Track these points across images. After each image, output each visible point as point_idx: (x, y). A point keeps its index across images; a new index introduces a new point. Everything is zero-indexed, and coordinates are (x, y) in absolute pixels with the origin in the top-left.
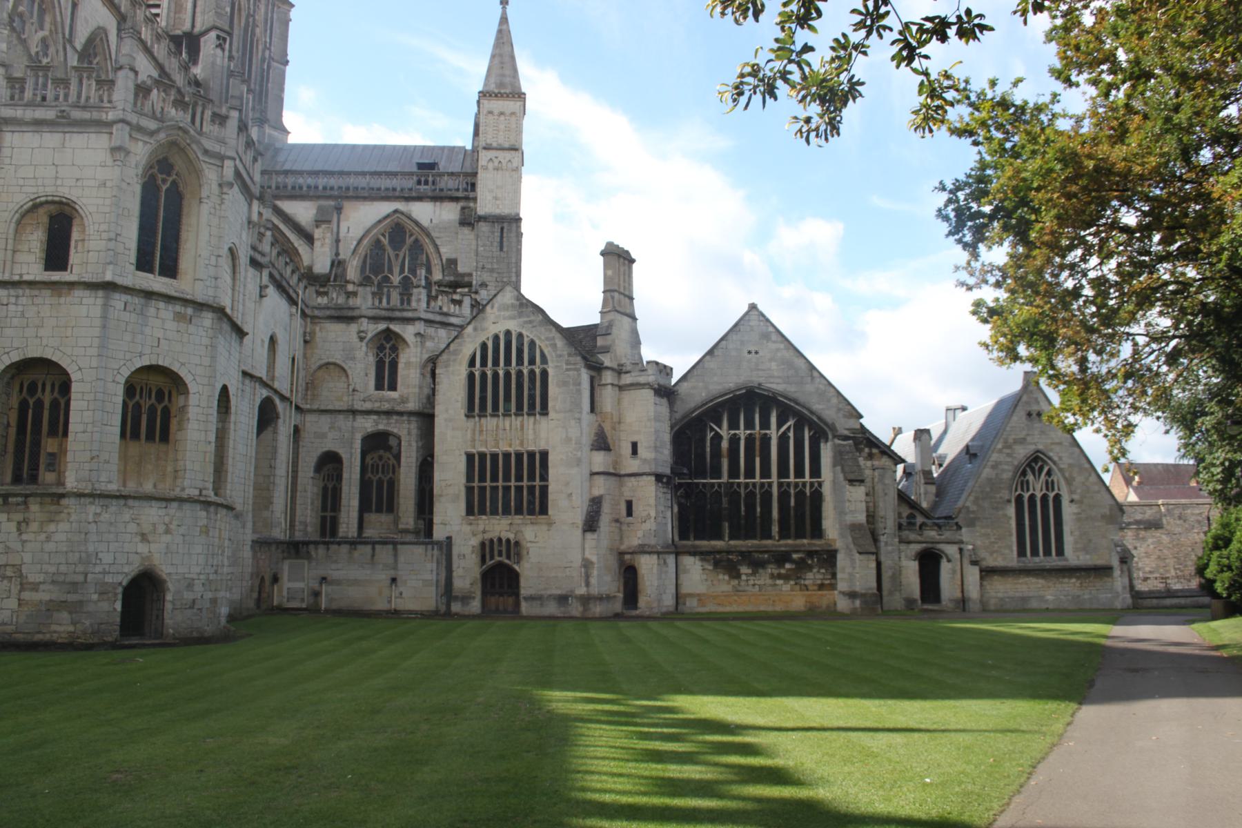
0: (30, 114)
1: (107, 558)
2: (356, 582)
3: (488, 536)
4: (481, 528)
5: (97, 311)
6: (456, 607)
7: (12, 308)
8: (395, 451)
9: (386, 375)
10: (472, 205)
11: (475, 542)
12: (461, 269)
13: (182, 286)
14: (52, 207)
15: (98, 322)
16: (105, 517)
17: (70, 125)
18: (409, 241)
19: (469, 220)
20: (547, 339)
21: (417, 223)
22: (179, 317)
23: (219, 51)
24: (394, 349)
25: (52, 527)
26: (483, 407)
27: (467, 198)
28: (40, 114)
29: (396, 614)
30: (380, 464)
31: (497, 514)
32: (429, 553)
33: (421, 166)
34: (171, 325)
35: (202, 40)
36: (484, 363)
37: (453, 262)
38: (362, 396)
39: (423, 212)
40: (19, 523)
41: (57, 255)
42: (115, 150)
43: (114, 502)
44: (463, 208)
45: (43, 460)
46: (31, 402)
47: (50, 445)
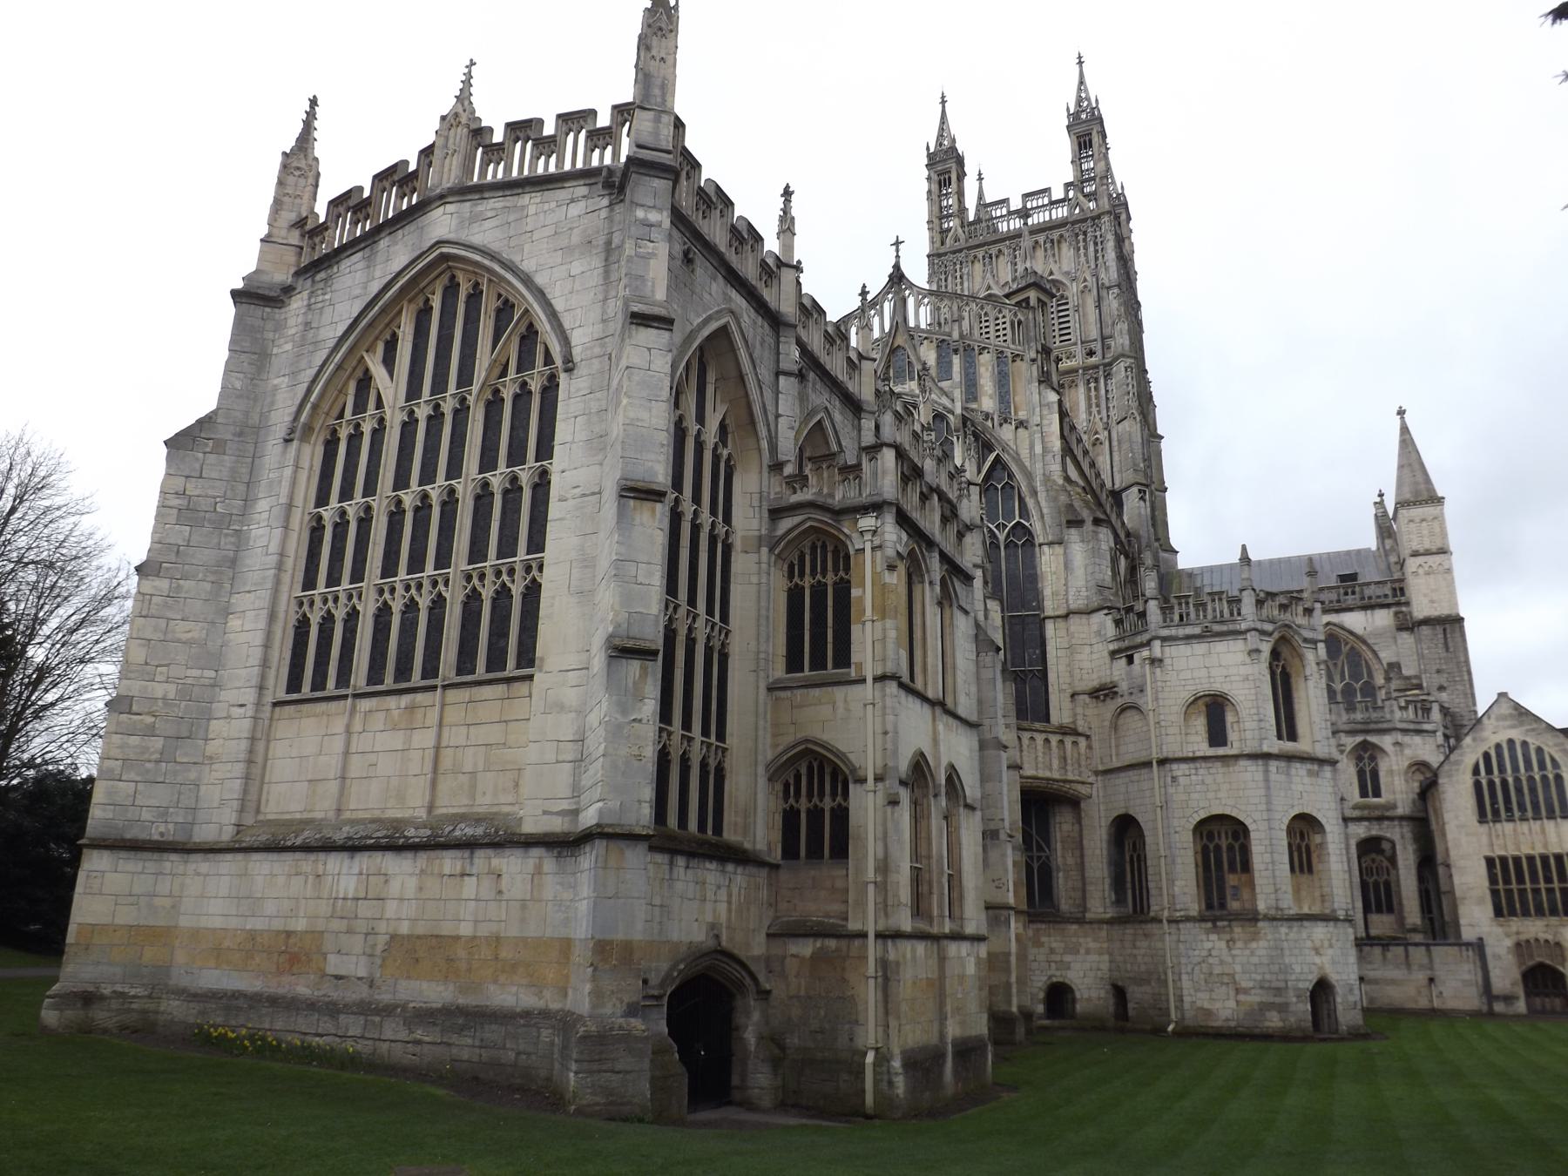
0: (1182, 632)
1: (1297, 969)
2: (1393, 982)
3: (1523, 937)
4: (1514, 929)
5: (1259, 776)
6: (1499, 1007)
7: (1193, 777)
8: (1388, 853)
9: (1369, 782)
10: (1404, 609)
11: (1509, 943)
12: (1406, 672)
13: (1303, 745)
14: (1207, 699)
15: (1262, 784)
16: (1292, 936)
17: (1212, 636)
18: (1345, 649)
19: (1407, 624)
20: (1556, 745)
21: (1351, 633)
22: (1310, 773)
23: (1142, 503)
24: (1373, 758)
25: (1254, 945)
26: (1496, 813)
27: (1398, 604)
28: (1189, 630)
29: (1433, 1013)
30: (1374, 866)
31: (1530, 915)
32: (1464, 953)
33: (1343, 578)
34: (1307, 780)
35: (1124, 495)
36: (1489, 771)
37: (1394, 667)
38: (1351, 804)
39: (1355, 621)
40: (1228, 941)
41: (1217, 735)
42: (1250, 653)
43: (1295, 924)
44: (1396, 614)
45: (1229, 892)
46: (1211, 847)
47: (1232, 880)
